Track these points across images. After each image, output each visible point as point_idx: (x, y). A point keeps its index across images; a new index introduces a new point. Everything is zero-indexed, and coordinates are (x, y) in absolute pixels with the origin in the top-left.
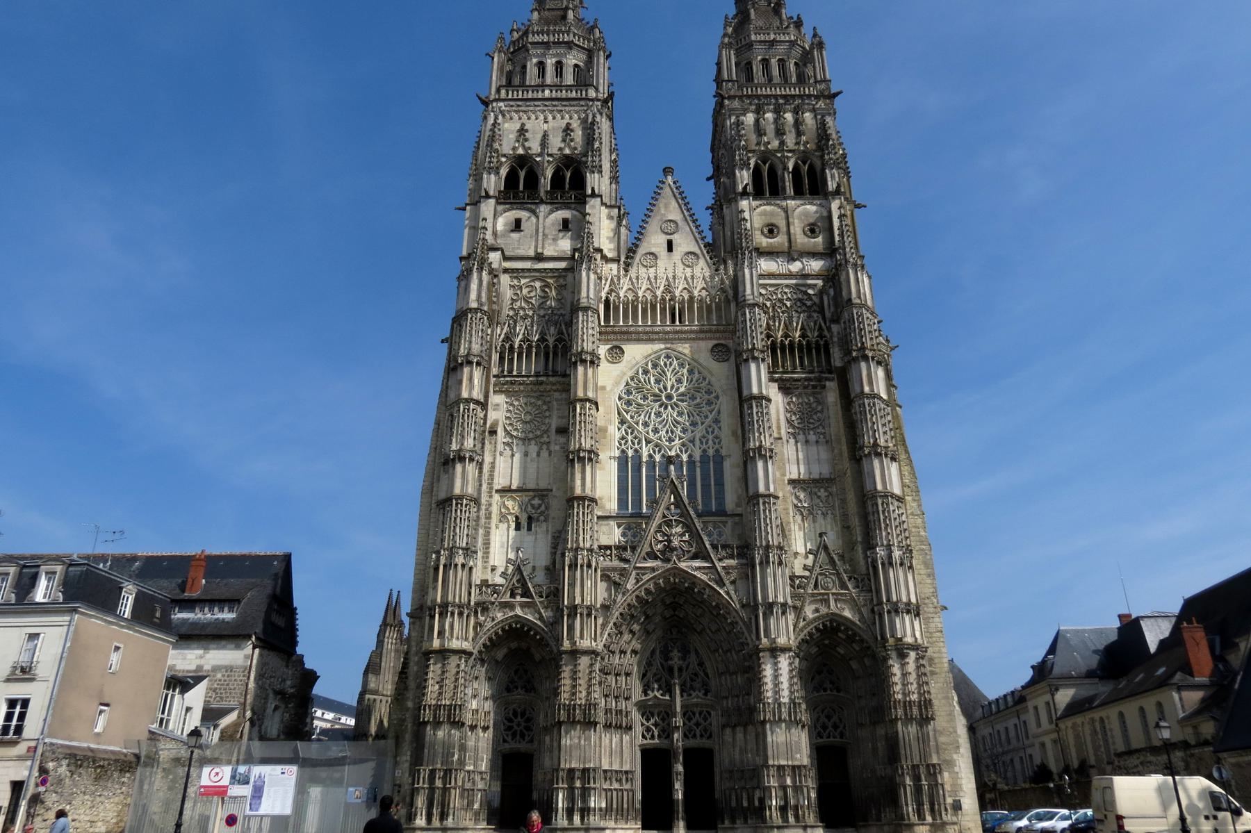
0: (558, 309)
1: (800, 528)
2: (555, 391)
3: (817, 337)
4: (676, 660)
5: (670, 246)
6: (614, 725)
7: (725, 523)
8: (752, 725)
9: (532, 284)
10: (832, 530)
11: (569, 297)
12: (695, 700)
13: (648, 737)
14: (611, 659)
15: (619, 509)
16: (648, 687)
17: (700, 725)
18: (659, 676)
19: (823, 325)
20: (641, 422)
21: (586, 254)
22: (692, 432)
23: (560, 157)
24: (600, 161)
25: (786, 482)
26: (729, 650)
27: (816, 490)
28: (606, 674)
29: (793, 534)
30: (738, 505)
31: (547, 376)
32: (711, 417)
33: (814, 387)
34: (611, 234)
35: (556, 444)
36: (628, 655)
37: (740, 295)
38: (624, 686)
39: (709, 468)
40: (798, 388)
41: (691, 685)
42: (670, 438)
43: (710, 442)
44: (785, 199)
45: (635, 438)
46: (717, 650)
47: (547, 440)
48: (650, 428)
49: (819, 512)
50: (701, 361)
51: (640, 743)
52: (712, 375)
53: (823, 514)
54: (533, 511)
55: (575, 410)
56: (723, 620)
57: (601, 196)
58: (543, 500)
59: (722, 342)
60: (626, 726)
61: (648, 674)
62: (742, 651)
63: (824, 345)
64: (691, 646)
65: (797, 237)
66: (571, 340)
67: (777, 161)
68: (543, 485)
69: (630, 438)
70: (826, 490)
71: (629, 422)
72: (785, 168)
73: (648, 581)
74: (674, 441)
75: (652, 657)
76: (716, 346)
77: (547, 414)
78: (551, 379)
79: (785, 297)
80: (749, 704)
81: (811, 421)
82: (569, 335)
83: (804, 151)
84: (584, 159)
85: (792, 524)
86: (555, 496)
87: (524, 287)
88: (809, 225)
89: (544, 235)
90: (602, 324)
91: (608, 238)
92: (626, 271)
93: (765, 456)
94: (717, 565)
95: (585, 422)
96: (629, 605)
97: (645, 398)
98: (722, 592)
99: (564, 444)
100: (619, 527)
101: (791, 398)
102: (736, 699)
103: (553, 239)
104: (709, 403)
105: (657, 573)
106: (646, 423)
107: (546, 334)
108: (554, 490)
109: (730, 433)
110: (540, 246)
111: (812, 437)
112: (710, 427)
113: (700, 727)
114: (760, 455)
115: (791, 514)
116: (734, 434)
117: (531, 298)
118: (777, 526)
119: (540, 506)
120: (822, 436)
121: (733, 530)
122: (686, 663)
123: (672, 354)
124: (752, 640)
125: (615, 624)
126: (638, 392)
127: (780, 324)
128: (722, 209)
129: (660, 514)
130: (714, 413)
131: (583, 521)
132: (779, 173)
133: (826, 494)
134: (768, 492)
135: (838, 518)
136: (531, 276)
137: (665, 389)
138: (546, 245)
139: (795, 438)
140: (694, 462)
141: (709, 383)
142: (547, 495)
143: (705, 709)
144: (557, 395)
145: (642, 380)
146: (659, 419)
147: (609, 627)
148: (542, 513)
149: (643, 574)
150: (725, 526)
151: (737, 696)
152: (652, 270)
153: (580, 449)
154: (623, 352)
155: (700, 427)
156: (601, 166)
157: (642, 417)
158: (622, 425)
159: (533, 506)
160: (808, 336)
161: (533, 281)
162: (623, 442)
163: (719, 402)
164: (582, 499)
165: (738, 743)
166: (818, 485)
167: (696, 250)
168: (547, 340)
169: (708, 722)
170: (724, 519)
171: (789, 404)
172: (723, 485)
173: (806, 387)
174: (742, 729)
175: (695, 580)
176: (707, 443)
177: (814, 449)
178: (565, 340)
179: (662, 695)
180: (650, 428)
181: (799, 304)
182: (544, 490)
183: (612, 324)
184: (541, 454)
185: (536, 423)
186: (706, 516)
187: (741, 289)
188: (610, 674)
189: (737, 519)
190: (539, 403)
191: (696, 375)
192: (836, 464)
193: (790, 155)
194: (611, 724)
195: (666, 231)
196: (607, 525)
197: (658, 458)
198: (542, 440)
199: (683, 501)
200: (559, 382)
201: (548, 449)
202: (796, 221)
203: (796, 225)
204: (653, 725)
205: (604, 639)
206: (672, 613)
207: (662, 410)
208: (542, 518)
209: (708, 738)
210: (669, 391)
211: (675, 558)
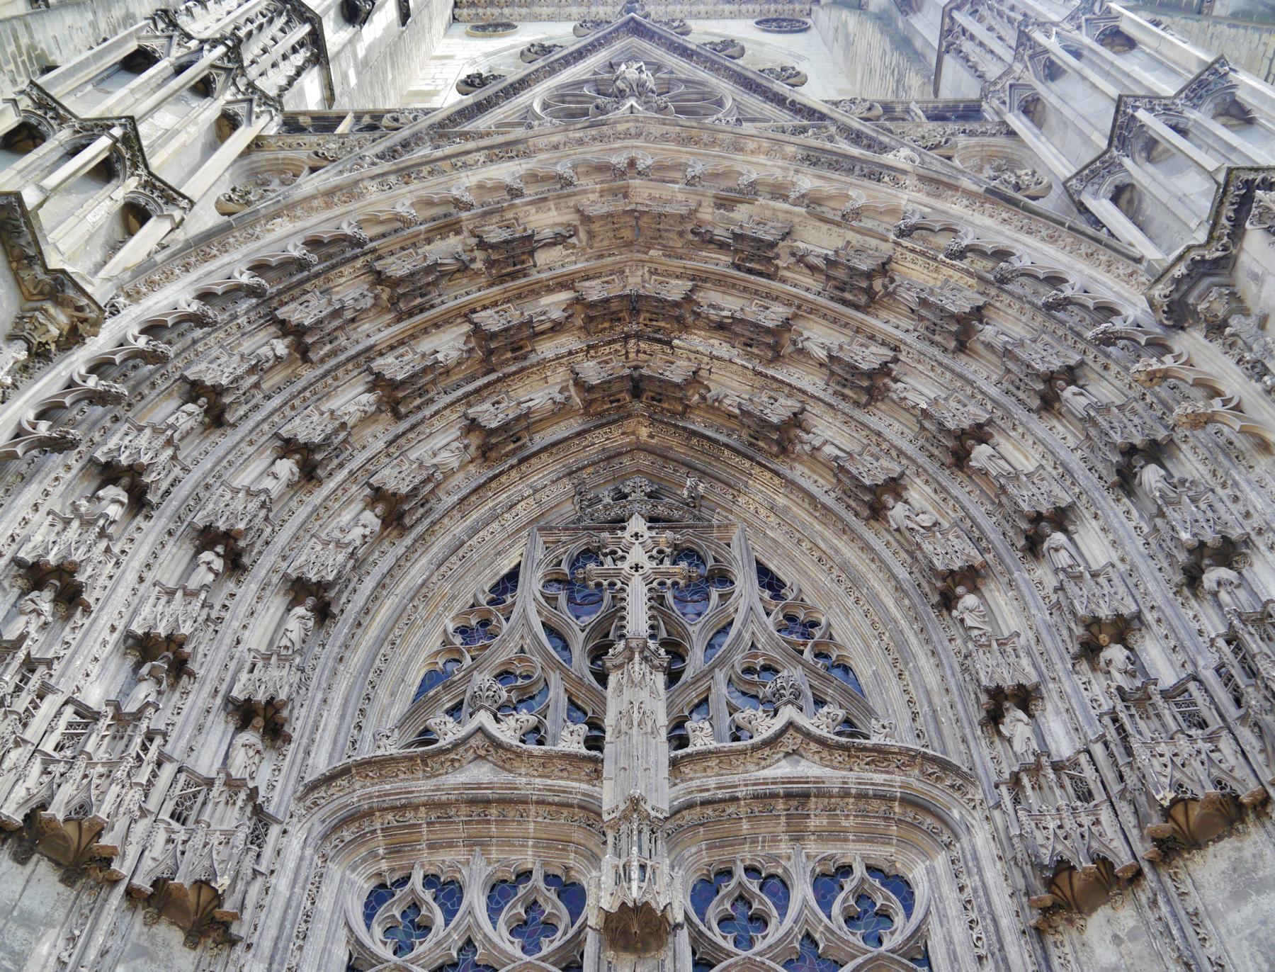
4: (637, 554)
12: (783, 769)
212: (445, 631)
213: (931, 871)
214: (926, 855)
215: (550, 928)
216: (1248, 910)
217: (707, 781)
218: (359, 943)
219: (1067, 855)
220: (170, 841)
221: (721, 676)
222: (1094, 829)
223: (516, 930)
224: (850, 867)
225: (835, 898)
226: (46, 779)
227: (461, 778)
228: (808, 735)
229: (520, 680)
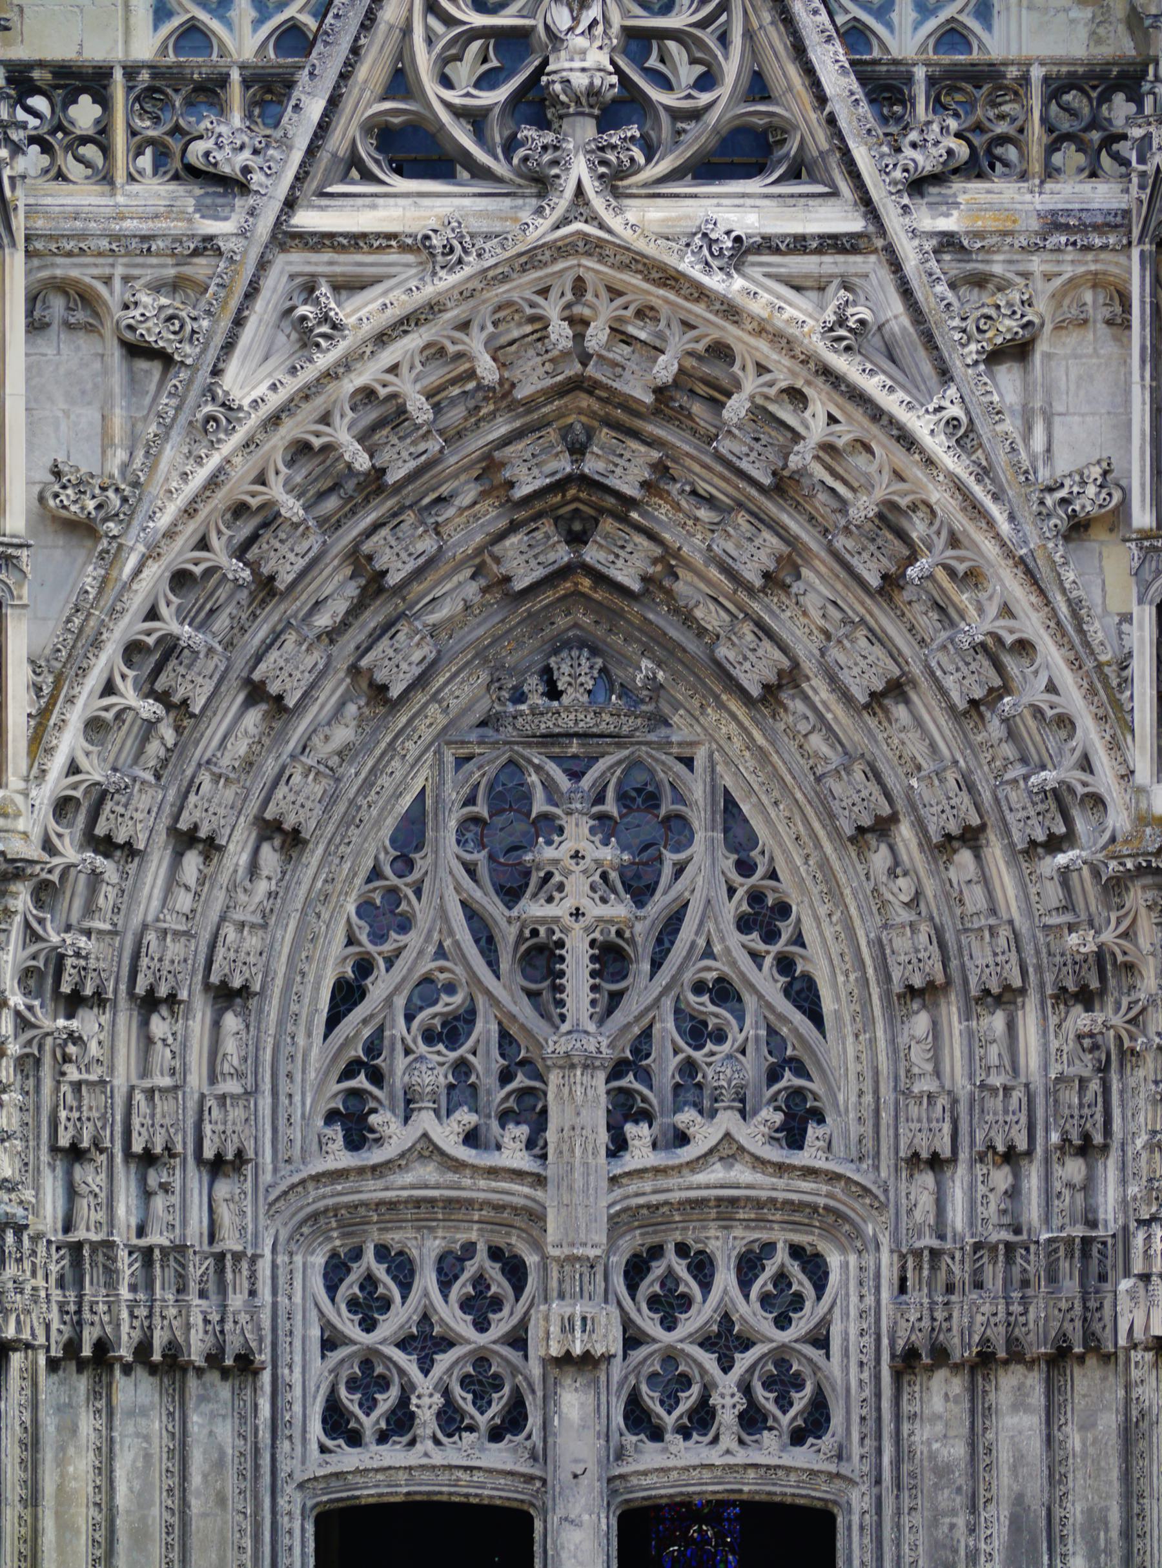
6: (125, 1352)
8: (1107, 1359)
12: (716, 1173)
13: (370, 1423)
14: (107, 897)
16: (377, 1077)
17: (746, 1344)
18: (454, 1002)
26: (971, 837)
28: (73, 1003)
36: (237, 854)
38: (196, 1079)
41: (689, 1067)
46: (883, 827)
51: (315, 1465)
56: (927, 621)
60: (214, 1359)
61: (379, 987)
62: (1054, 844)
64: (697, 790)
73: (382, 339)
75: (405, 863)
80: (1093, 1224)
94: (894, 221)
96: (240, 510)
98: (920, 425)
102: (1001, 1178)
105: (448, 280)
113: (743, 1361)
122: (659, 904)
124: (1128, 775)
125: (133, 651)
143: (782, 1238)
147: (94, 680)
149: (347, 286)
151: (1010, 1157)
165: (1004, 1482)
169: (802, 1324)
174: (1035, 1382)
175: (732, 334)
179: (472, 1138)
188: (99, 1000)
194: (102, 1346)
204: (403, 1344)
205: (57, 764)
206: (562, 554)
209: (798, 1438)
211: (580, 169)
212: (348, 921)
213: (845, 1266)
214: (843, 1250)
215: (496, 1304)
216: (1016, 1420)
217: (645, 1192)
218: (329, 1322)
219: (917, 1344)
220: (206, 1321)
221: (668, 1004)
222: (945, 1325)
223: (466, 1305)
224: (801, 1148)
225: (757, 1277)
226: (136, 1323)
227: (409, 1178)
228: (741, 1149)
229: (445, 998)
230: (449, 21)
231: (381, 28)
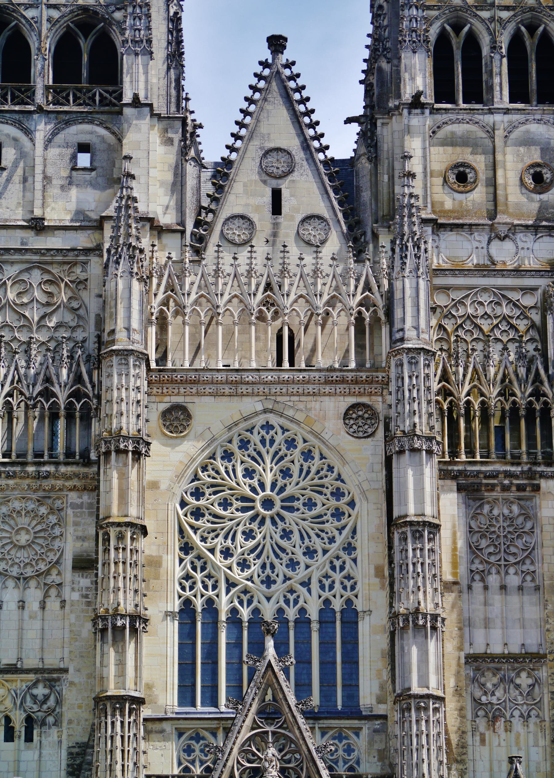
0: (73, 329)
1: (483, 741)
2: (70, 490)
3: (531, 395)
5: (277, 209)
7: (357, 732)
9: (25, 277)
10: (536, 745)
11: (93, 306)
15: (180, 704)
19: (542, 372)
20: (219, 548)
21: (124, 244)
22: (307, 567)
23: (72, 12)
24: (149, 28)
25: (463, 660)
27: (513, 675)
29: (470, 750)
30: (381, 700)
31: (57, 464)
32: (339, 539)
33: (520, 488)
34: (169, 177)
35: (73, 589)
37: (397, 325)
39: (335, 632)
40: (492, 490)
42: (268, 577)
43: (337, 585)
44: (491, 112)
45: (209, 576)
47: (58, 580)
48: (234, 560)
49: (517, 713)
50: (326, 436)
52: (344, 461)
53: (522, 716)
54: (36, 708)
55: (107, 540)
57: (151, 106)
58: (51, 687)
59: (364, 400)
63: (541, 409)
65: (510, 190)
66: (99, 397)
67: (480, 28)
68: (52, 661)
69: (198, 576)
70: (529, 676)
71: (198, 548)
72: (494, 47)
74: (275, 582)
76: (354, 407)
77: (57, 531)
78: (63, 469)
79: (480, 312)
81: (513, 550)
82: (93, 387)
83: (532, 9)
84: (118, 15)
85: (470, 734)
86: (72, 683)
87: (9, 283)
88: (532, 166)
89: (47, 179)
90: (153, 365)
91: (162, 183)
92: (197, 252)
93: (424, 626)
95: (124, 563)
97: (225, 504)
99: (87, 588)
100: (180, 735)
101: (481, 506)
103: (62, 187)
104: (338, 514)
106: (228, 549)
107: (52, 384)
108: (71, 671)
109: (372, 572)
110: (38, 203)
111: (513, 580)
112: (338, 558)
114: (416, 625)
115: (469, 716)
116: (379, 571)
117: (23, 305)
118: (440, 748)
119: (46, 698)
120: (529, 578)
121: (371, 743)
123: (274, 420)
126: (215, 493)
127: (466, 369)
128: (375, 125)
129: (248, 722)
130: (345, 532)
131: (122, 737)
132: (485, 51)
133: (530, 681)
134: (425, 691)
135: (547, 724)
136: (27, 262)
137: (262, 485)
138: (49, 200)
139: (482, 580)
140: (309, 621)
141: (339, 478)
142: (58, 679)
144: (73, 497)
145: (222, 470)
146: (251, 543)
148: (51, 712)
150: (357, 735)
152: (243, 254)
153: (116, 614)
154: (189, 417)
155: (321, 558)
156: (149, 41)
157: (220, 539)
158: (187, 554)
159: (34, 697)
160: (514, 395)
161: (28, 270)
162: (187, 584)
163: (354, 513)
164: (121, 699)
166: (516, 665)
167: (322, 209)
168: (54, 395)
170: (355, 723)
171: (474, 517)
172: (357, 663)
173: (506, 488)
176: (331, 587)
177: (514, 599)
178: (86, 396)
180: (234, 560)
181: (504, 326)
182: (51, 671)
183: (169, 366)
184: (48, 605)
185: (37, 548)
186: (326, 718)
187: (398, 313)
189: (377, 723)
190: (43, 510)
191: (316, 463)
192: (548, 630)
193: (505, 15)
195: (270, 170)
196: (162, 731)
197: (245, 613)
198: (49, 580)
199: (286, 700)
200: (76, 475)
201: (59, 595)
202: (509, 158)
203: (509, 165)
207: (254, 526)
208: (51, 719)
210: (268, 492)
230: (243, 765)
231: (227, 767)
